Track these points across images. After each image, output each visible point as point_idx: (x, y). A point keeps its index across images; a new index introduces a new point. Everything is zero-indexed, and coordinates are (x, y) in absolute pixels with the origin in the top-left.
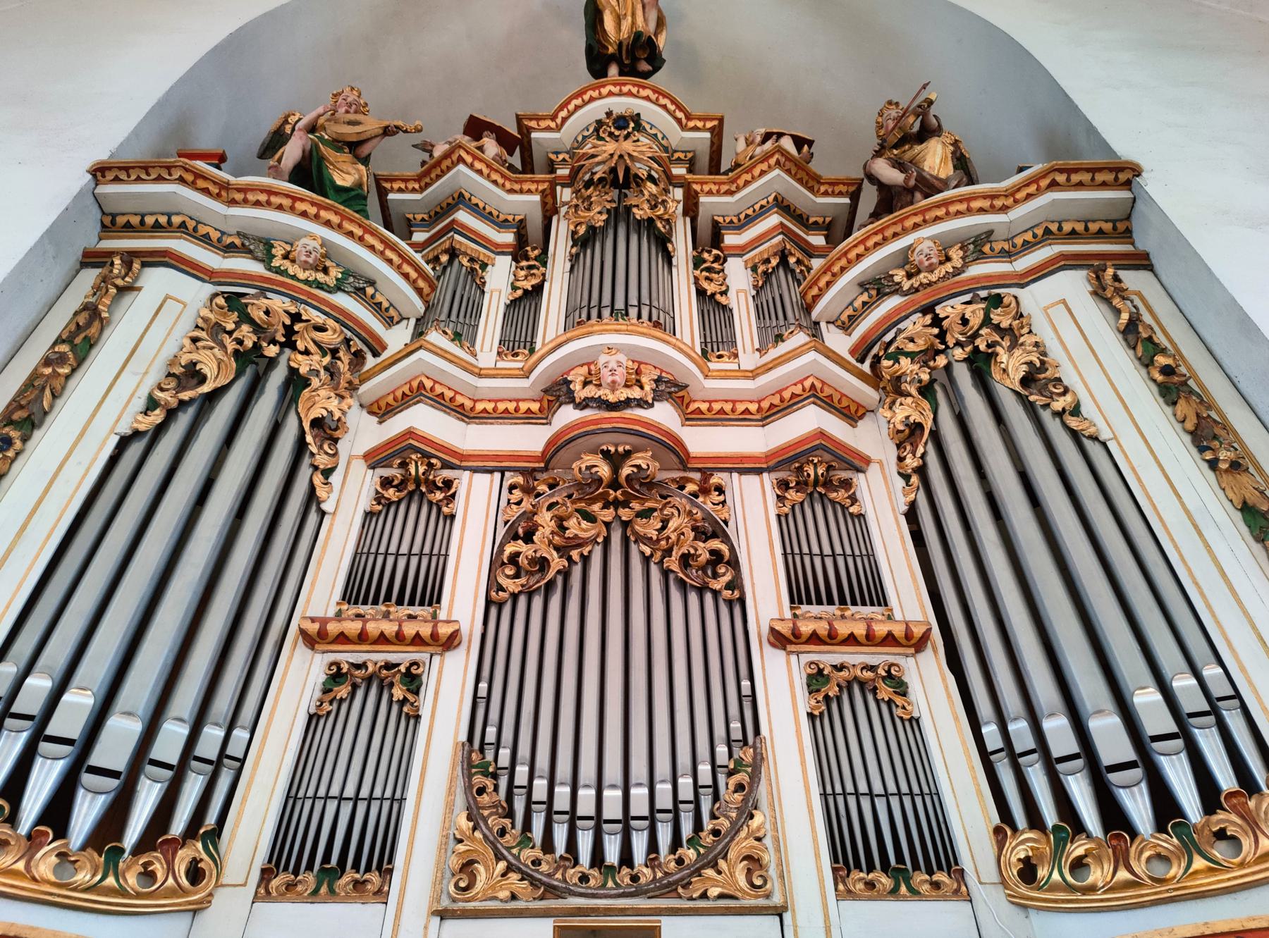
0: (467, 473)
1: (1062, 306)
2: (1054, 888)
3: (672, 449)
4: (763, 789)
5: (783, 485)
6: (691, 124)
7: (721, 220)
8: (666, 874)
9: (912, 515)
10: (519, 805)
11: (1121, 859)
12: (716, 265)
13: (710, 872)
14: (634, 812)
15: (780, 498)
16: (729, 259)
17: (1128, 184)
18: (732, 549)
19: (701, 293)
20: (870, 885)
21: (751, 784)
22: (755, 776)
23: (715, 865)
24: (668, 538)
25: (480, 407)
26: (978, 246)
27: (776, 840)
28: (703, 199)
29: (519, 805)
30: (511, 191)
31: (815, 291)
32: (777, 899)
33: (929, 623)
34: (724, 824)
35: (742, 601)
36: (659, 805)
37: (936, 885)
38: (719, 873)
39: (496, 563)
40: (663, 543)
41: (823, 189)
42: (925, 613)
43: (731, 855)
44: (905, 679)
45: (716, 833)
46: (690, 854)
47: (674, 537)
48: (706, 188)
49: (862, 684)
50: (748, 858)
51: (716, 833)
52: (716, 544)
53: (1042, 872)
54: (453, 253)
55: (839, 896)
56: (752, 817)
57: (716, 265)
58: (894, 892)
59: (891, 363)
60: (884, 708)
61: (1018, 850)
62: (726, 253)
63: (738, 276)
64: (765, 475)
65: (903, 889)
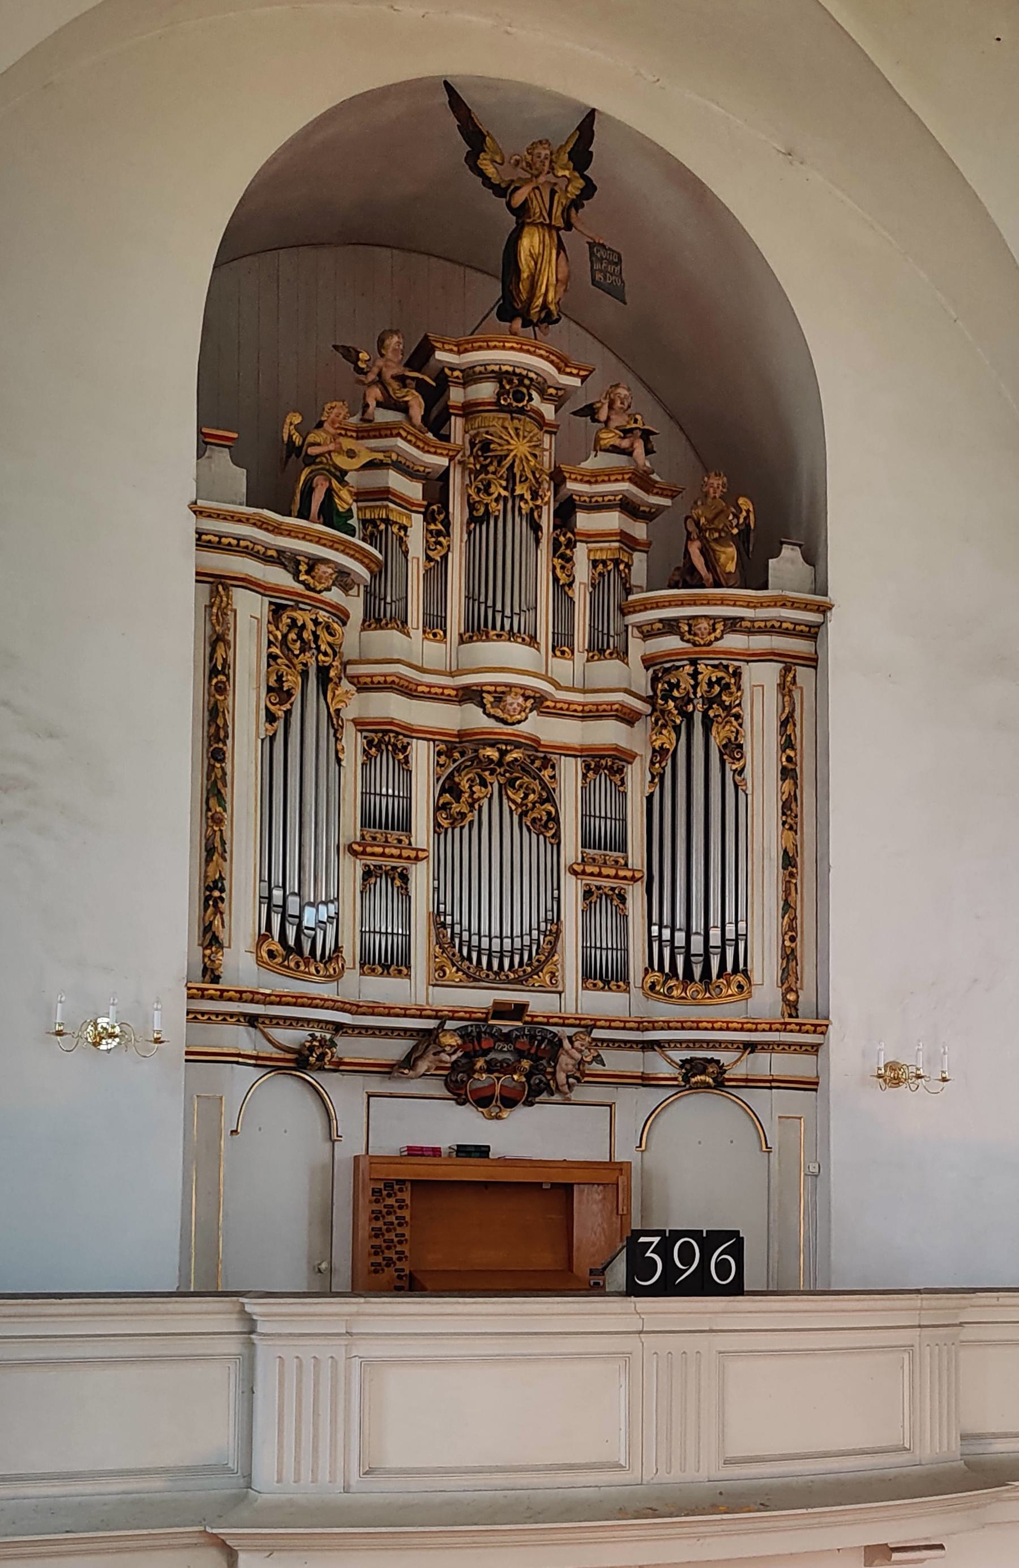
0: (415, 740)
1: (761, 688)
2: (660, 994)
3: (534, 744)
4: (559, 944)
5: (588, 767)
6: (568, 370)
7: (577, 498)
8: (519, 976)
9: (650, 799)
10: (457, 941)
11: (685, 990)
12: (568, 552)
13: (536, 977)
14: (505, 949)
15: (585, 776)
16: (578, 544)
17: (824, 612)
18: (557, 811)
19: (556, 579)
20: (595, 985)
21: (555, 942)
22: (557, 938)
23: (537, 974)
24: (527, 806)
25: (420, 689)
26: (733, 625)
27: (562, 966)
28: (570, 485)
29: (457, 941)
30: (429, 452)
31: (631, 609)
32: (560, 989)
33: (643, 873)
34: (543, 958)
35: (559, 844)
36: (515, 946)
37: (619, 987)
38: (539, 977)
39: (438, 809)
40: (524, 808)
41: (655, 491)
42: (643, 866)
43: (544, 971)
44: (626, 896)
45: (538, 961)
46: (529, 969)
47: (530, 805)
48: (573, 476)
49: (607, 896)
50: (551, 972)
51: (538, 961)
52: (548, 807)
53: (657, 988)
54: (387, 521)
55: (583, 989)
56: (553, 956)
57: (568, 552)
58: (603, 989)
59: (663, 702)
60: (614, 908)
61: (649, 980)
62: (578, 538)
63: (582, 571)
64: (579, 759)
65: (606, 987)
